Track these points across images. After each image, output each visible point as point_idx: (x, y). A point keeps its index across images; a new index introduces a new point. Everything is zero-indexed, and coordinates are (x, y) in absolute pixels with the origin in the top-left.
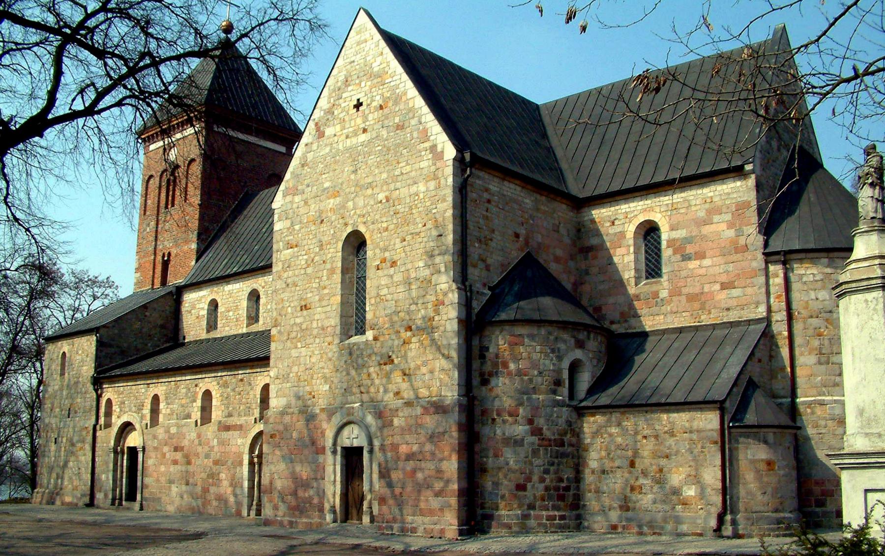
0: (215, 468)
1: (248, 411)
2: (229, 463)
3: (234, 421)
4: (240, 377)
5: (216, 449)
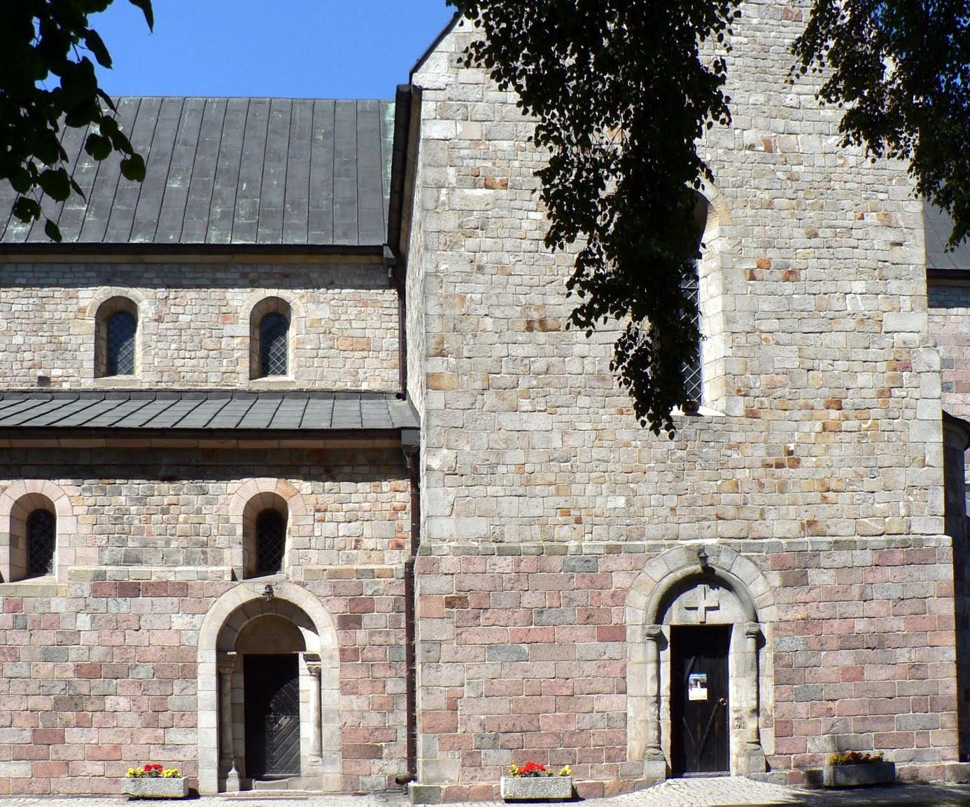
1: (202, 549)
2: (143, 672)
3: (154, 571)
5: (87, 638)
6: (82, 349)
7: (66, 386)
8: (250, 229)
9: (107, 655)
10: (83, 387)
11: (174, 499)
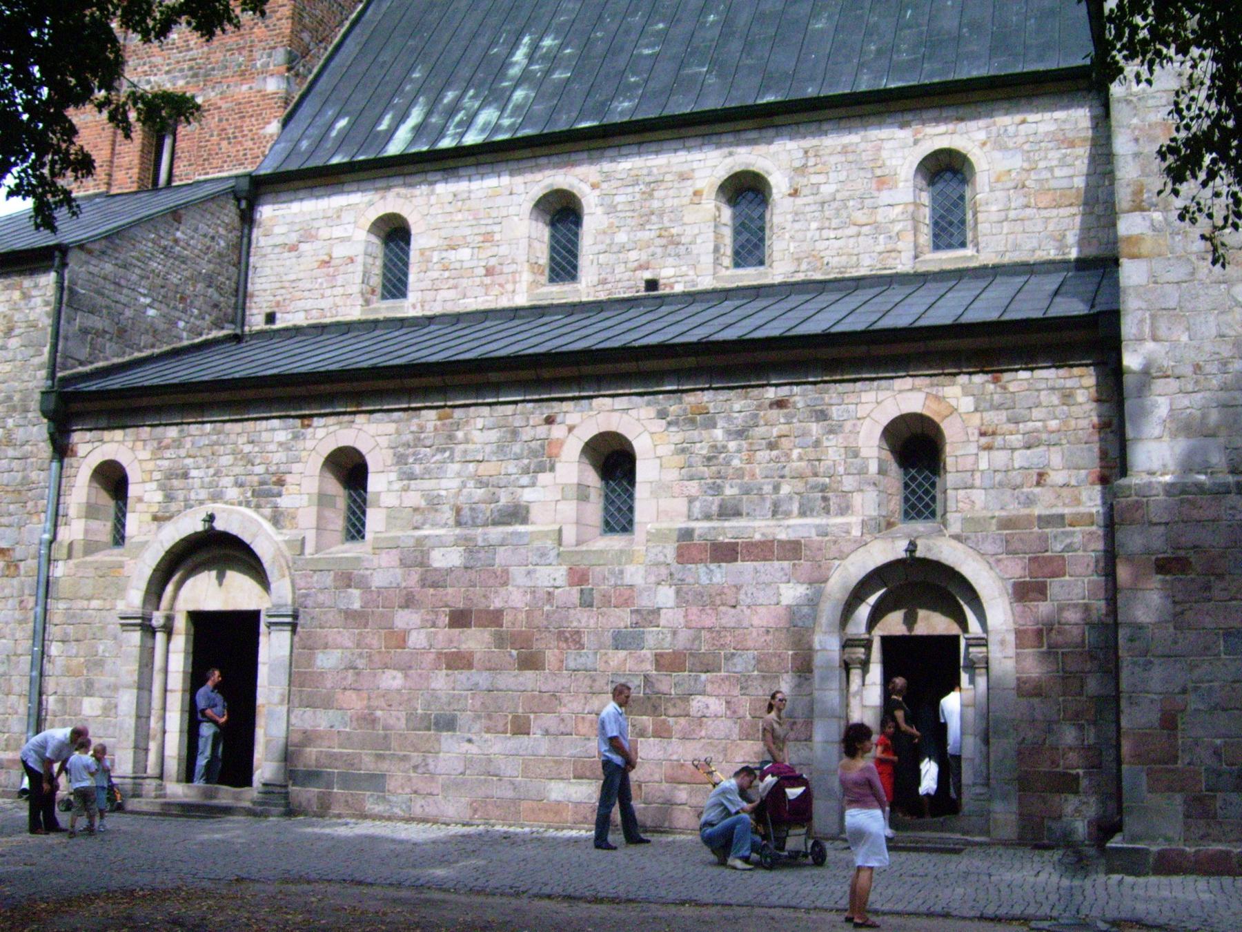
0: (665, 684)
2: (742, 664)
3: (757, 527)
4: (771, 393)
6: (699, 241)
7: (678, 288)
8: (913, 65)
9: (694, 640)
10: (700, 287)
11: (784, 429)
